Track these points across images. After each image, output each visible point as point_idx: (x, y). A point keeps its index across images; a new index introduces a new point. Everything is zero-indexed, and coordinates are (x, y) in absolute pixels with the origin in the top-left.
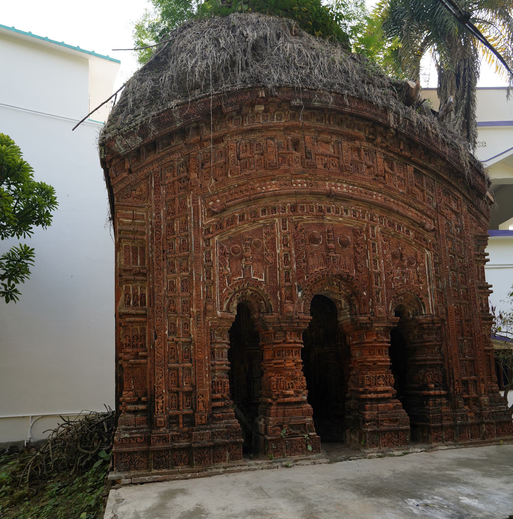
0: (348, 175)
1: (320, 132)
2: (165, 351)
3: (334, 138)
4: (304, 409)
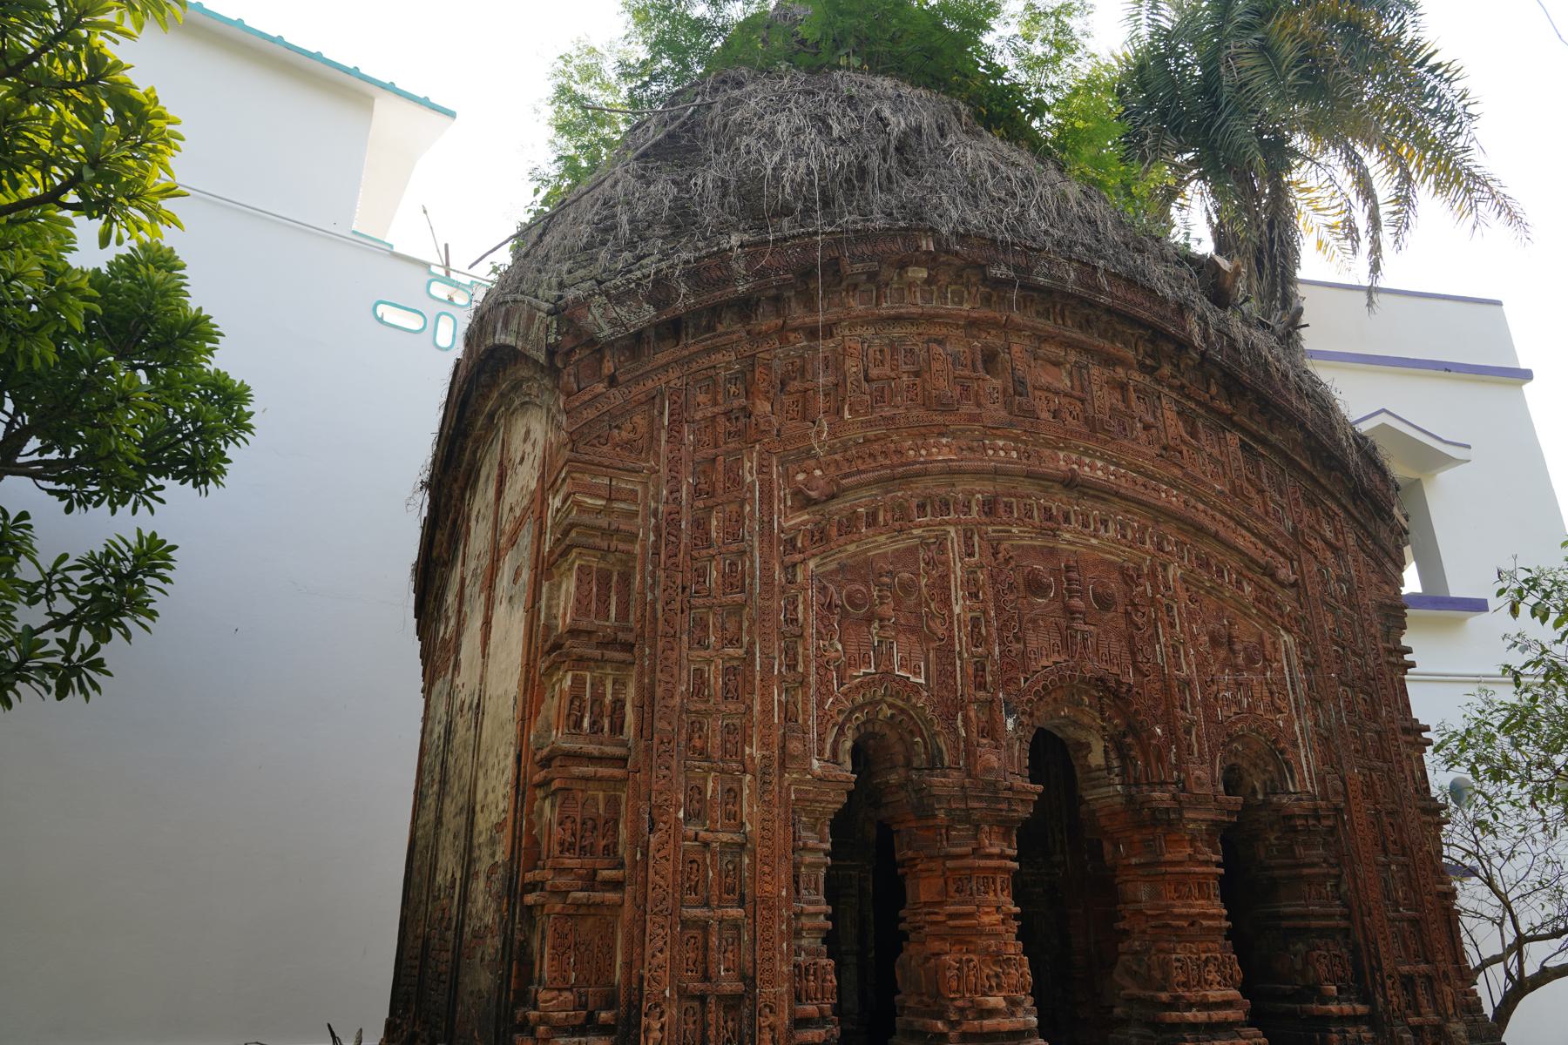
0: (1106, 442)
1: (1043, 338)
3: (1073, 357)
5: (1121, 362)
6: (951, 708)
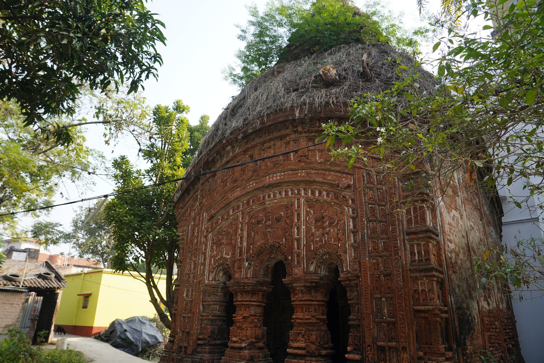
0: (278, 167)
2: (182, 306)
4: (241, 354)
5: (287, 135)
6: (234, 262)
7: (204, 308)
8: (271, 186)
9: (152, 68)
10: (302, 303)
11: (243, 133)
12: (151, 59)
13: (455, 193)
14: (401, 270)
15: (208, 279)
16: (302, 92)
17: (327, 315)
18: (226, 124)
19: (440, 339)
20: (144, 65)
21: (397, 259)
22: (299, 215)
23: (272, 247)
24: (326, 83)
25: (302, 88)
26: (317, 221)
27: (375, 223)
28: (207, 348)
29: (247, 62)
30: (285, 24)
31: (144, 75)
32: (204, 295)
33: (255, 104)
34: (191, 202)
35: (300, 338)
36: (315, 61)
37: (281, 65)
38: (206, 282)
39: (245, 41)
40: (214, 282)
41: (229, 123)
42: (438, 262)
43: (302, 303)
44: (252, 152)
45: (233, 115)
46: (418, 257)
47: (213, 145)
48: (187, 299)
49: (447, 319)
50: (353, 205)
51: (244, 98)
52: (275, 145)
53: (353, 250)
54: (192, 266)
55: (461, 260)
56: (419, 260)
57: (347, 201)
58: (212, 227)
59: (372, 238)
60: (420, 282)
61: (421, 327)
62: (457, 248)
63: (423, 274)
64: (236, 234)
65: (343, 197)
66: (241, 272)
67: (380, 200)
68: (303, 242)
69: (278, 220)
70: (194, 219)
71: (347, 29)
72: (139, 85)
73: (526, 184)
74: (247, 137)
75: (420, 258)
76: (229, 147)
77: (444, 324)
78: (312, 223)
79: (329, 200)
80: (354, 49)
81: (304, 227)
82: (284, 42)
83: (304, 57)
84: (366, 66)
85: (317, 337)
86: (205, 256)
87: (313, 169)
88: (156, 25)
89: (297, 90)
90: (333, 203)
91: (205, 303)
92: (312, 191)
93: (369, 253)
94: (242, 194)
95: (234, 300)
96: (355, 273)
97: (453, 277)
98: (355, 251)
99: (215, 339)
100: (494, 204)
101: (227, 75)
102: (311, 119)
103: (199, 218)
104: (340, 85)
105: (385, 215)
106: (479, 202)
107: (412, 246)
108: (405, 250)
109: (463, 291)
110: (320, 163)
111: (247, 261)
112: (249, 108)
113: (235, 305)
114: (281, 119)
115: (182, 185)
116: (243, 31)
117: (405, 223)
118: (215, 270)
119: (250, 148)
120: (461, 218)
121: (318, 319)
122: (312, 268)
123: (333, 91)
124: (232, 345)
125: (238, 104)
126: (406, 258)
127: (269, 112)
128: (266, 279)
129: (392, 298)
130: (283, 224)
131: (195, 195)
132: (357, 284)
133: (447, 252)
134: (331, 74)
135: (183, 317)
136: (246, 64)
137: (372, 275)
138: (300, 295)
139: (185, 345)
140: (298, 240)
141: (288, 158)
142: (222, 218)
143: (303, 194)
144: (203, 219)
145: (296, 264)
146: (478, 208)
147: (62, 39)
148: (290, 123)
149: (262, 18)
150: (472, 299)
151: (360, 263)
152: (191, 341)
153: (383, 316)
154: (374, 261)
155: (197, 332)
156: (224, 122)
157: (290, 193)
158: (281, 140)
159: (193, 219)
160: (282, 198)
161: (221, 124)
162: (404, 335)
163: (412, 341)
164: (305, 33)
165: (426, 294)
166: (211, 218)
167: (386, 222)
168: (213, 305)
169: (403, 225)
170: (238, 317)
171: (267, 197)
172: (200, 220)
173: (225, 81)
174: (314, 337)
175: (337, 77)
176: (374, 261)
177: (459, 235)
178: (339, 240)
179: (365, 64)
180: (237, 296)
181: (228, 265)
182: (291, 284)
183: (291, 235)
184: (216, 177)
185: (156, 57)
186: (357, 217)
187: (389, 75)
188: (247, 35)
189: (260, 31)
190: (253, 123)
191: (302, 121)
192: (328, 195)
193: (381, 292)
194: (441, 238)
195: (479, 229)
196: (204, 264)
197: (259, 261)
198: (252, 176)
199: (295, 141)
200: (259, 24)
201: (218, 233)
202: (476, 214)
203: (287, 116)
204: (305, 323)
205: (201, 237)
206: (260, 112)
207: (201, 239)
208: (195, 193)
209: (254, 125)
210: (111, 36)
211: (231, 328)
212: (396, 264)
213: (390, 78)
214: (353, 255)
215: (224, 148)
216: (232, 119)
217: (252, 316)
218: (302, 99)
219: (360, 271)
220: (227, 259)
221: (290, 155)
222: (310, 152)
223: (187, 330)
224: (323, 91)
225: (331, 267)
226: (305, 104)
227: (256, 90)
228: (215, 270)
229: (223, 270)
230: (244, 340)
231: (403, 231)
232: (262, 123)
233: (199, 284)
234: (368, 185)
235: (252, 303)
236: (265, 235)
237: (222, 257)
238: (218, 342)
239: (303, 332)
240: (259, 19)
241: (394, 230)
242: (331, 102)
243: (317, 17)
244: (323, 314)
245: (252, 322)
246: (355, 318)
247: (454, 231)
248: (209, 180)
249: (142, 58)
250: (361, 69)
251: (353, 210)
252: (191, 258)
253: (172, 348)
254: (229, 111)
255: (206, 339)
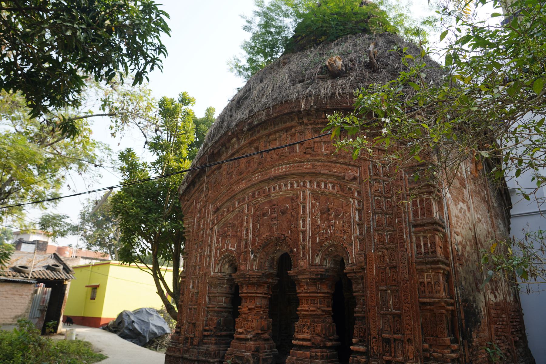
0: (284, 159)
1: (269, 135)
2: (188, 298)
4: (247, 345)
5: (292, 127)
6: (239, 254)
7: (210, 299)
8: (277, 178)
9: (157, 59)
10: (308, 295)
11: (248, 125)
12: (155, 50)
13: (463, 186)
14: (406, 263)
15: (214, 271)
16: (308, 84)
17: (332, 307)
18: (231, 116)
19: (446, 331)
20: (148, 56)
21: (403, 251)
22: (304, 207)
23: (278, 239)
24: (332, 74)
25: (308, 79)
26: (322, 213)
27: (381, 215)
28: (213, 339)
29: (253, 53)
30: (291, 14)
31: (149, 67)
32: (210, 287)
33: (261, 95)
34: (197, 194)
35: (305, 329)
36: (322, 52)
37: (287, 56)
38: (212, 273)
39: (250, 32)
40: (219, 274)
41: (234, 115)
42: (444, 254)
43: (308, 295)
44: (257, 144)
45: (238, 107)
46: (425, 250)
47: (219, 137)
48: (193, 290)
49: (453, 311)
50: (359, 197)
51: (250, 90)
52: (280, 137)
53: (359, 242)
54: (198, 258)
55: (468, 252)
56: (425, 253)
57: (352, 193)
58: (217, 220)
59: (378, 230)
60: (425, 274)
61: (426, 319)
62: (464, 241)
63: (429, 266)
64: (241, 226)
65: (349, 189)
66: (246, 264)
67: (386, 192)
68: (309, 234)
69: (283, 212)
70: (200, 211)
71: (354, 19)
72: (144, 77)
73: (534, 176)
74: (252, 129)
75: (426, 251)
76: (235, 139)
77: (449, 317)
78: (317, 215)
79: (335, 192)
80: (361, 39)
81: (310, 219)
82: (290, 33)
83: (310, 48)
84: (373, 56)
85: (322, 329)
86: (211, 248)
87: (319, 161)
88: (160, 15)
89: (302, 81)
90: (338, 196)
91: (211, 295)
92: (317, 183)
93: (374, 246)
94: (247, 186)
95: (240, 292)
96: (361, 265)
97: (460, 269)
98: (360, 243)
99: (221, 331)
100: (502, 196)
101: (233, 67)
102: (317, 110)
103: (205, 210)
104: (346, 76)
105: (391, 207)
106: (487, 194)
107: (418, 239)
108: (411, 242)
109: (469, 284)
110: (326, 155)
111: (252, 253)
112: (254, 100)
113: (240, 297)
114: (287, 111)
115: (187, 177)
116: (248, 21)
117: (411, 215)
118: (221, 262)
119: (255, 140)
120: (469, 210)
121: (323, 311)
122: (317, 260)
123: (339, 82)
124: (238, 336)
125: (243, 96)
126: (412, 250)
127: (274, 103)
128: (272, 271)
129: (397, 291)
130: (289, 216)
131: (201, 188)
132: (363, 276)
133: (453, 245)
134: (337, 65)
135: (189, 308)
136: (252, 56)
137: (378, 268)
138: (306, 287)
139: (192, 336)
140: (304, 233)
141: (293, 150)
142: (228, 210)
143: (308, 186)
144: (208, 211)
145: (301, 256)
146: (486, 201)
147: (66, 31)
148: (295, 115)
149: (268, 8)
150: (479, 291)
151: (365, 256)
152: (198, 332)
153: (388, 308)
154: (380, 253)
155: (203, 323)
156: (230, 114)
157: (295, 185)
158: (287, 132)
159: (199, 212)
160: (288, 190)
161: (226, 116)
162: (409, 327)
163: (417, 333)
164: (311, 24)
165: (432, 287)
166: (217, 210)
167: (392, 214)
168: (219, 296)
169: (409, 217)
170: (244, 308)
171: (272, 189)
172: (205, 213)
173: (230, 73)
174: (319, 329)
175: (344, 68)
176: (380, 253)
177: (467, 227)
178: (345, 232)
179: (372, 54)
180: (242, 288)
181: (234, 257)
182: (297, 276)
183: (297, 227)
184: (222, 169)
185: (161, 49)
186: (363, 209)
187: (396, 66)
188: (252, 25)
189: (266, 21)
190: (258, 115)
191: (308, 113)
192: (333, 187)
193: (386, 284)
194: (447, 230)
195: (487, 222)
196: (210, 256)
197: (264, 253)
198: (257, 169)
199: (301, 133)
200: (265, 14)
201: (224, 225)
202: (483, 206)
203: (293, 108)
204: (311, 315)
205: (207, 230)
206: (265, 104)
207: (206, 231)
208: (201, 185)
209: (260, 117)
210: (116, 27)
211: (237, 320)
212: (402, 256)
213: (397, 69)
214: (359, 247)
215: (229, 140)
216: (237, 111)
217: (257, 307)
218: (308, 91)
219: (366, 263)
220: (232, 251)
221: (296, 147)
222: (316, 144)
223: (193, 322)
224: (329, 82)
225: (336, 259)
226: (311, 96)
227: (261, 81)
228: (221, 262)
229: (229, 262)
230: (250, 332)
231: (409, 223)
232: (268, 115)
233: (205, 276)
234: (373, 177)
235: (258, 295)
236: (270, 227)
237: (227, 249)
238: (224, 333)
239: (308, 324)
240: (265, 9)
241: (400, 223)
242: (337, 93)
243: (324, 7)
244: (328, 306)
245: (257, 314)
246: (360, 310)
247: (461, 223)
248: (215, 172)
249: (147, 49)
250: (368, 59)
251: (359, 202)
252: (197, 251)
253: (178, 339)
254: (234, 102)
255: (212, 330)
